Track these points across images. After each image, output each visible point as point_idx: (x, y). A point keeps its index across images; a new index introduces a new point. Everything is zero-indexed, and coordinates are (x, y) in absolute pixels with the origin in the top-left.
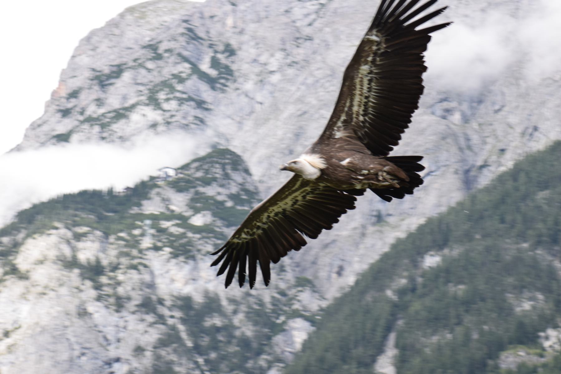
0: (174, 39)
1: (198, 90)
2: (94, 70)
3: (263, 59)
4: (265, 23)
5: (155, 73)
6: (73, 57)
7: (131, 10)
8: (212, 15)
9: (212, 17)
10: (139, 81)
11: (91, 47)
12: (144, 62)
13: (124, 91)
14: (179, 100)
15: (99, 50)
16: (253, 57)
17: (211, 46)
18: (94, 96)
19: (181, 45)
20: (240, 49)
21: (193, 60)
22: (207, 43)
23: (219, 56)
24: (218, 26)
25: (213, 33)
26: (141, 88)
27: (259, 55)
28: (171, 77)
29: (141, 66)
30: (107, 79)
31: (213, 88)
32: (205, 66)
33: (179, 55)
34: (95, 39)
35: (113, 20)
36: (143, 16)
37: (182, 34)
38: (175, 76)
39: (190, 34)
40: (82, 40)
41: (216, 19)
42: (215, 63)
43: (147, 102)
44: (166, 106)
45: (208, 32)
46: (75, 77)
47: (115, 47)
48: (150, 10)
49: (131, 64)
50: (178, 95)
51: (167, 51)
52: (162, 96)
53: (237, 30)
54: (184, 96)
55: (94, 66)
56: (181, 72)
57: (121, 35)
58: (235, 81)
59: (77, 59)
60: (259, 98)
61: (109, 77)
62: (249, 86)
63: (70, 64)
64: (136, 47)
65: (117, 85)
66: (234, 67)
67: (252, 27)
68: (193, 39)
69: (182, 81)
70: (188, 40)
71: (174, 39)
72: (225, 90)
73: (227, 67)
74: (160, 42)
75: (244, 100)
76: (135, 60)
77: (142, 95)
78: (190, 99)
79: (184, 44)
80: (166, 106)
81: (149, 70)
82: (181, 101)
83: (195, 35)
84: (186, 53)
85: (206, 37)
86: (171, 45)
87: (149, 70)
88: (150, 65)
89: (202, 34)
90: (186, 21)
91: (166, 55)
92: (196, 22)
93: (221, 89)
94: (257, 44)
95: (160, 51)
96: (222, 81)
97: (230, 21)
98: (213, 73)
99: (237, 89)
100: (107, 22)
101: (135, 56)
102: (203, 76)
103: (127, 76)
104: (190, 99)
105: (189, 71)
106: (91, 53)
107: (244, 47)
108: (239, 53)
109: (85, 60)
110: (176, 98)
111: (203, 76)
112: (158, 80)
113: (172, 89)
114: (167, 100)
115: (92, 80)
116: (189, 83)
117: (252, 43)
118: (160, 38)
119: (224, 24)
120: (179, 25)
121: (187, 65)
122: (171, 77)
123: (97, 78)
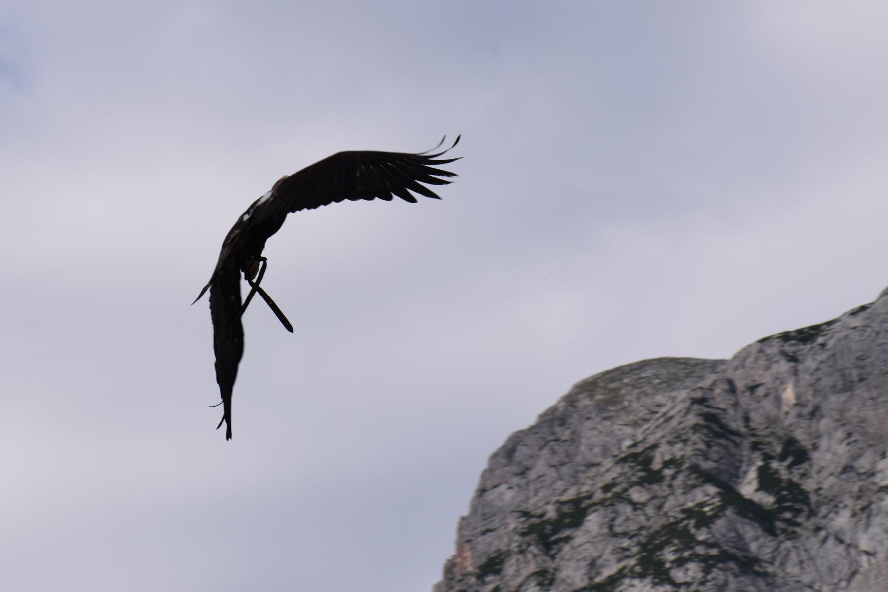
0: (679, 438)
1: (740, 537)
2: (526, 514)
3: (864, 463)
4: (861, 391)
5: (650, 510)
6: (482, 492)
7: (588, 387)
8: (752, 384)
9: (752, 389)
10: (618, 530)
11: (515, 469)
12: (625, 490)
13: (592, 551)
14: (701, 561)
15: (532, 475)
16: (844, 461)
17: (755, 447)
18: (532, 568)
19: (698, 450)
20: (815, 447)
21: (724, 478)
22: (747, 443)
23: (775, 465)
24: (767, 405)
25: (757, 419)
26: (626, 543)
27: (856, 457)
28: (681, 516)
29: (622, 497)
30: (555, 531)
31: (770, 531)
32: (748, 488)
33: (694, 468)
34: (522, 452)
35: (553, 410)
36: (614, 399)
37: (696, 428)
38: (689, 513)
39: (715, 427)
40: (495, 456)
41: (760, 391)
42: (767, 480)
43: (638, 569)
44: (679, 575)
45: (747, 419)
46: (489, 531)
47: (563, 464)
48: (627, 385)
49: (599, 495)
50: (700, 550)
51: (666, 464)
52: (669, 555)
53: (806, 411)
54: (714, 552)
55: (524, 507)
56: (702, 505)
57: (575, 439)
58: (812, 513)
59: (491, 496)
60: (864, 543)
61: (558, 525)
62: (842, 520)
63: (474, 509)
64: (608, 463)
65: (577, 541)
66: (809, 485)
67: (835, 400)
68: (718, 435)
69: (704, 521)
70: (707, 439)
71: (679, 438)
72: (794, 532)
73: (793, 487)
74: (655, 446)
75: (834, 551)
76: (606, 488)
77: (627, 557)
78: (725, 557)
79: (702, 446)
80: (679, 575)
81: (636, 506)
82: (708, 564)
83: (723, 426)
84: (706, 465)
85: (743, 430)
86: (678, 450)
87: (636, 506)
88: (637, 495)
89: (737, 424)
90: (702, 401)
91: (668, 472)
92: (721, 400)
93: (784, 531)
94: (849, 435)
95: (656, 465)
96: (788, 515)
97: (789, 394)
98: (767, 500)
99: (818, 529)
100: (541, 416)
101: (608, 478)
103: (593, 521)
104: (725, 557)
105: (717, 501)
106: (515, 480)
107: (824, 443)
108: (815, 456)
109: (505, 496)
110: (694, 557)
111: (748, 508)
112: (656, 524)
113: (688, 540)
114: (680, 563)
115: (524, 535)
116: (720, 525)
117: (840, 434)
118: (651, 440)
119: (778, 400)
120: (688, 411)
121: (712, 490)
122: (681, 516)
123: (532, 529)
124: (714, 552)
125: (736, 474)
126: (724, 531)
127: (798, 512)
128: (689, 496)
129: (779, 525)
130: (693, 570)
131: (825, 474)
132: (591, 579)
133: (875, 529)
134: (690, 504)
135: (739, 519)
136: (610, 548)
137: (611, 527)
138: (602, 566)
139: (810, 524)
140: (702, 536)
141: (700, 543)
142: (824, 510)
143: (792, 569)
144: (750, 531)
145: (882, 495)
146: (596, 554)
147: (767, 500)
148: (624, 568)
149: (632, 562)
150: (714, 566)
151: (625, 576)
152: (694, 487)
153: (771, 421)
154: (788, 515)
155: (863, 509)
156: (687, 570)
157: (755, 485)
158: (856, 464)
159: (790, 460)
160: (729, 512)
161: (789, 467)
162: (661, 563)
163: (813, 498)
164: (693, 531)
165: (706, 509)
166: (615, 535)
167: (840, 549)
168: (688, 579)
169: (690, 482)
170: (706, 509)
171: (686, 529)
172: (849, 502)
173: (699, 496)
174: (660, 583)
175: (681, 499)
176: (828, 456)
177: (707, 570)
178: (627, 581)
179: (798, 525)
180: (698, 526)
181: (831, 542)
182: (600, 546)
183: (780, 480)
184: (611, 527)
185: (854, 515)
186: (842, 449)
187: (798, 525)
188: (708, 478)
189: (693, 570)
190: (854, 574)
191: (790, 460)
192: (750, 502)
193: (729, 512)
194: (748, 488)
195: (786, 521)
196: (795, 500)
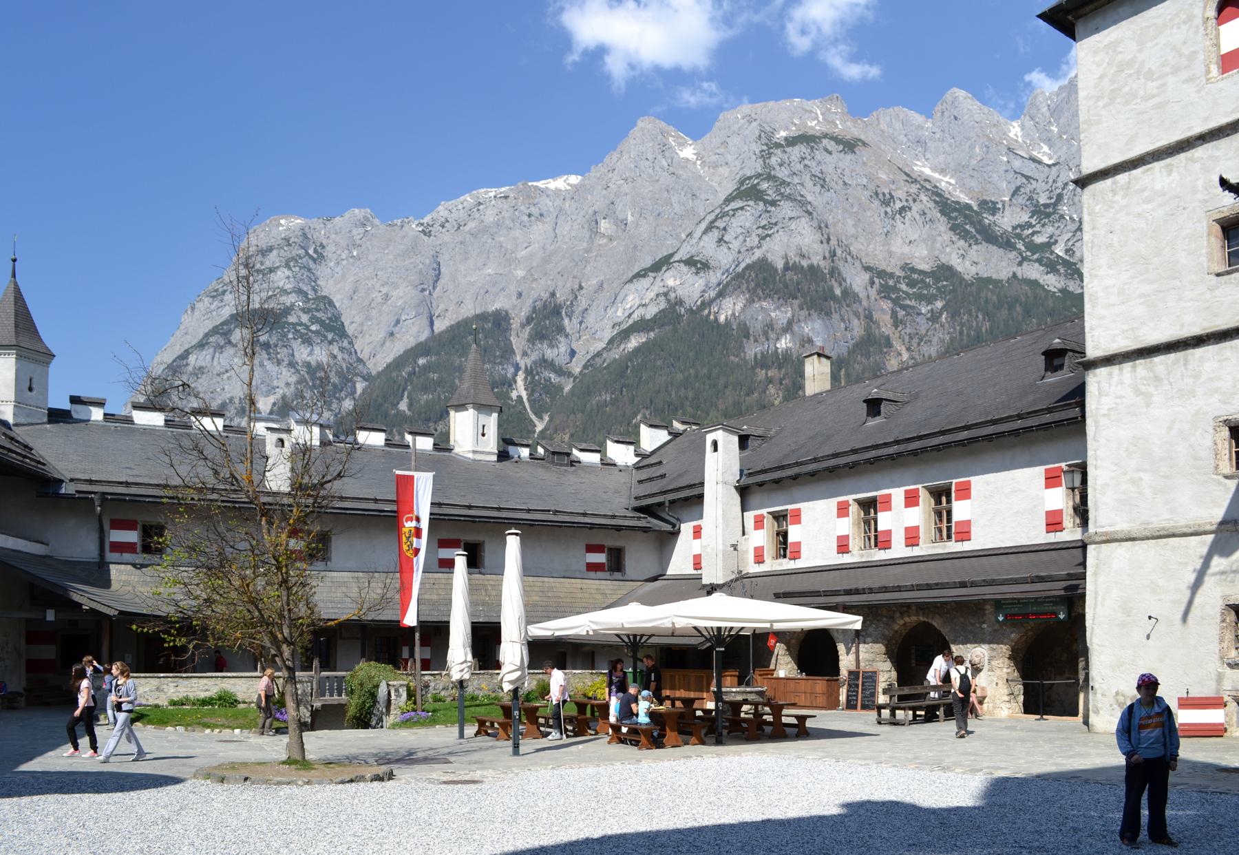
0: (296, 237)
3: (338, 252)
13: (273, 259)
25: (314, 236)
31: (315, 263)
32: (311, 252)
38: (297, 255)
42: (316, 251)
44: (293, 269)
52: (292, 264)
61: (266, 251)
62: (332, 264)
66: (325, 254)
69: (301, 258)
71: (296, 237)
73: (321, 254)
78: (305, 267)
86: (296, 240)
88: (286, 248)
89: (310, 237)
97: (323, 232)
98: (315, 256)
103: (275, 252)
104: (305, 267)
111: (310, 257)
112: (290, 256)
113: (297, 261)
114: (294, 266)
116: (304, 259)
125: (308, 248)
130: (297, 269)
133: (339, 268)
143: (319, 272)
144: (311, 262)
147: (315, 256)
153: (318, 237)
186: (334, 248)
188: (303, 248)
189: (297, 269)
194: (311, 252)
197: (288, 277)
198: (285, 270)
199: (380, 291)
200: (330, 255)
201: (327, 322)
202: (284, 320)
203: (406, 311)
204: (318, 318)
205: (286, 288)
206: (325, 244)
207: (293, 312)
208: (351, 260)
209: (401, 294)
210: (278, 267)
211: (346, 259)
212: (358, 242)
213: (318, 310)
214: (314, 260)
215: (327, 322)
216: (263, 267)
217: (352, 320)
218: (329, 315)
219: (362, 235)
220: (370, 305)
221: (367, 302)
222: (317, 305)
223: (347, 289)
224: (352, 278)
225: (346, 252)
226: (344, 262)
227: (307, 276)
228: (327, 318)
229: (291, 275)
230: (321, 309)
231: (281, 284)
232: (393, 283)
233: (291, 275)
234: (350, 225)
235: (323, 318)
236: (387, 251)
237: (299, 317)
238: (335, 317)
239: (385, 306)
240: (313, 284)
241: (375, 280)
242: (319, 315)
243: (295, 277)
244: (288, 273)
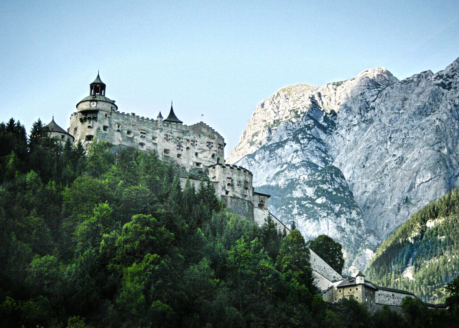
16: (345, 117)
23: (328, 116)
28: (304, 127)
31: (325, 133)
32: (321, 121)
44: (302, 142)
50: (308, 136)
54: (311, 137)
56: (309, 124)
58: (336, 129)
66: (336, 122)
78: (314, 138)
82: (309, 140)
96: (330, 129)
99: (337, 133)
102: (321, 127)
104: (314, 138)
114: (303, 138)
116: (313, 130)
121: (312, 121)
122: (304, 127)
124: (311, 137)
126: (314, 131)
127: (333, 128)
128: (307, 122)
129: (328, 131)
131: (340, 119)
132: (280, 140)
134: (306, 124)
135: (318, 129)
136: (286, 133)
137: (286, 128)
138: (283, 137)
139: (335, 132)
140: (308, 132)
141: (308, 134)
142: (339, 129)
145: (354, 127)
146: (282, 134)
148: (289, 138)
149: (291, 137)
150: (311, 140)
151: (289, 140)
152: (308, 120)
154: (330, 129)
155: (348, 130)
156: (304, 141)
157: (323, 120)
158: (348, 118)
159: (332, 115)
160: (316, 127)
161: (331, 117)
162: (298, 138)
163: (337, 126)
164: (307, 131)
165: (310, 126)
166: (287, 130)
167: (342, 138)
168: (304, 143)
169: (307, 119)
170: (310, 126)
171: (305, 130)
172: (345, 127)
173: (309, 122)
174: (298, 143)
175: (304, 122)
176: (341, 115)
177: (309, 141)
178: (289, 142)
179: (332, 132)
180: (308, 130)
181: (340, 136)
182: (283, 132)
183: (329, 120)
184: (286, 128)
185: (346, 131)
187: (332, 132)
190: (344, 145)
191: (332, 115)
192: (321, 125)
193: (316, 127)
195: (329, 130)
196: (332, 125)
197: (296, 151)
198: (293, 144)
199: (394, 155)
200: (341, 122)
201: (334, 193)
202: (289, 195)
203: (420, 173)
204: (324, 190)
205: (294, 162)
206: (336, 111)
207: (298, 187)
208: (363, 125)
209: (416, 156)
210: (286, 141)
211: (358, 124)
212: (372, 104)
213: (324, 183)
214: (324, 129)
215: (334, 193)
216: (269, 143)
217: (364, 190)
218: (336, 186)
219: (375, 97)
220: (383, 171)
221: (380, 169)
222: (323, 177)
223: (358, 156)
224: (364, 144)
225: (358, 117)
226: (356, 128)
227: (317, 147)
228: (335, 189)
229: (299, 148)
230: (328, 181)
231: (289, 159)
232: (409, 144)
233: (299, 148)
234: (363, 88)
235: (330, 190)
236: (401, 112)
237: (304, 191)
238: (342, 187)
239: (399, 170)
240: (323, 155)
241: (389, 143)
242: (325, 187)
243: (303, 150)
244: (296, 146)
